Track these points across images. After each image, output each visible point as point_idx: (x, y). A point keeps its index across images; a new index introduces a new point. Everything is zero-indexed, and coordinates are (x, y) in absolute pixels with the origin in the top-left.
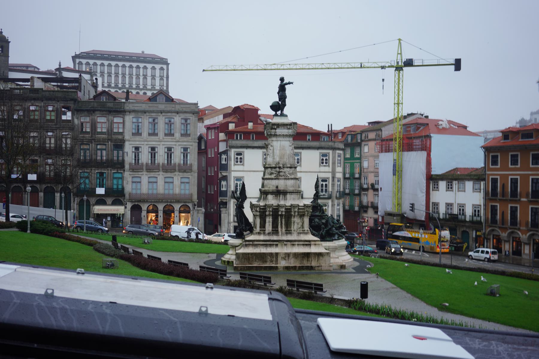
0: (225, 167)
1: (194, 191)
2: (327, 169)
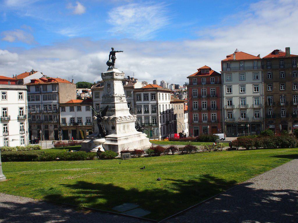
2: (21, 101)
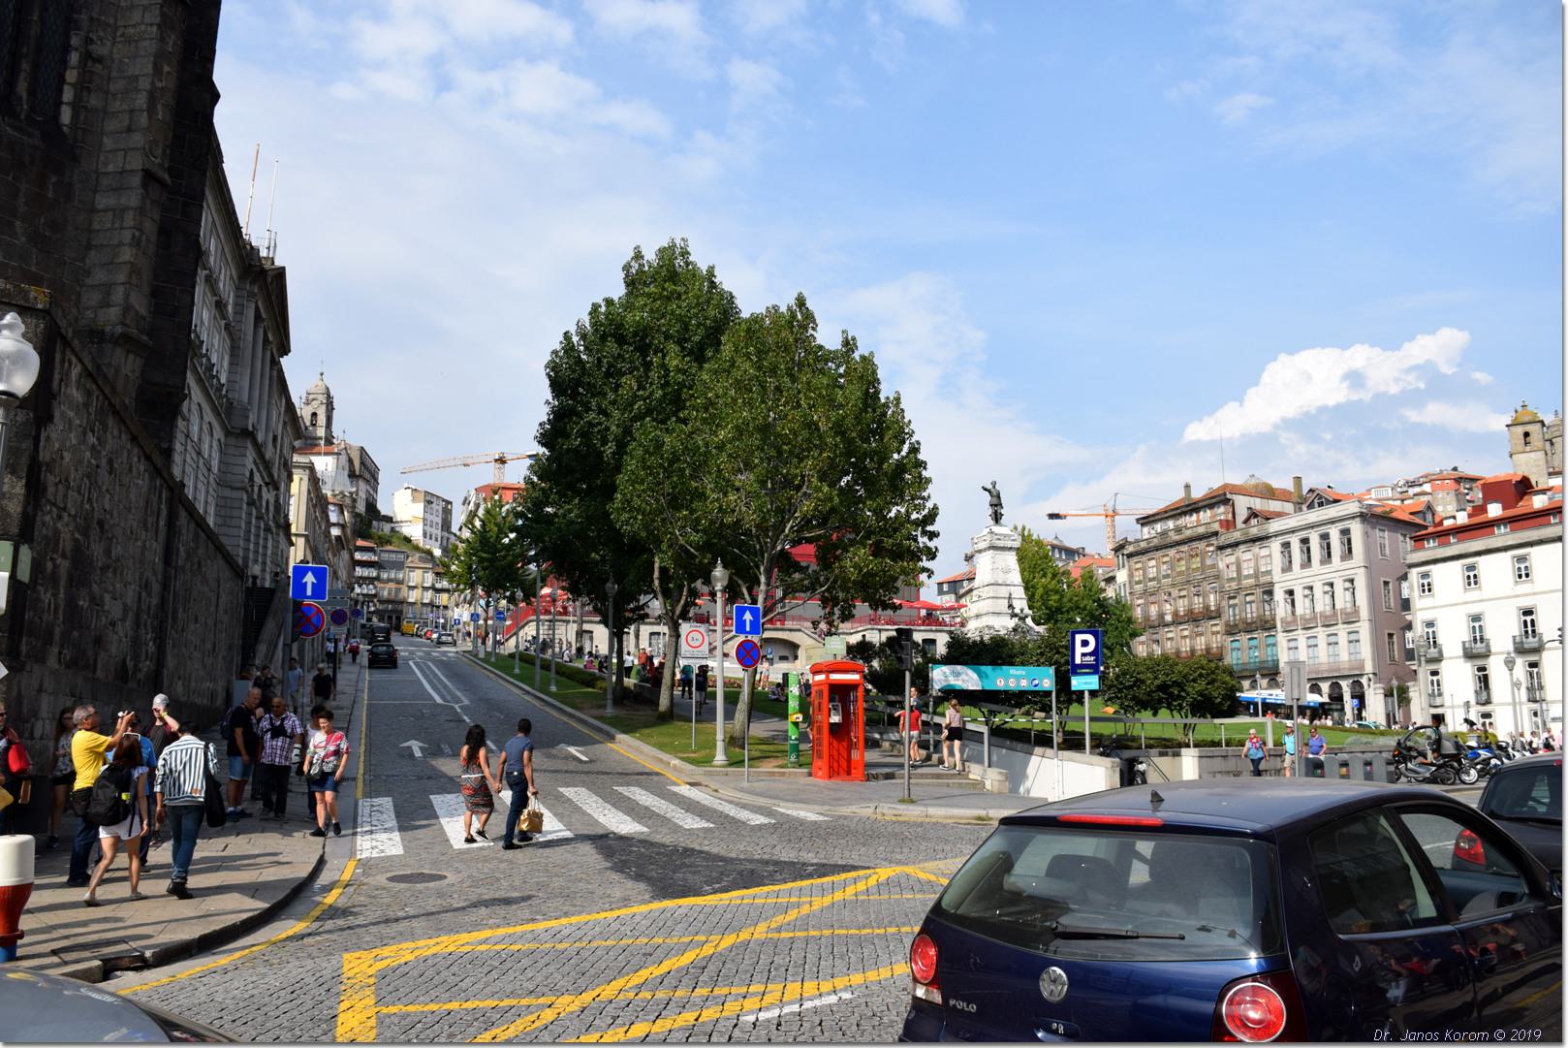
0: (1406, 605)
1: (1366, 651)
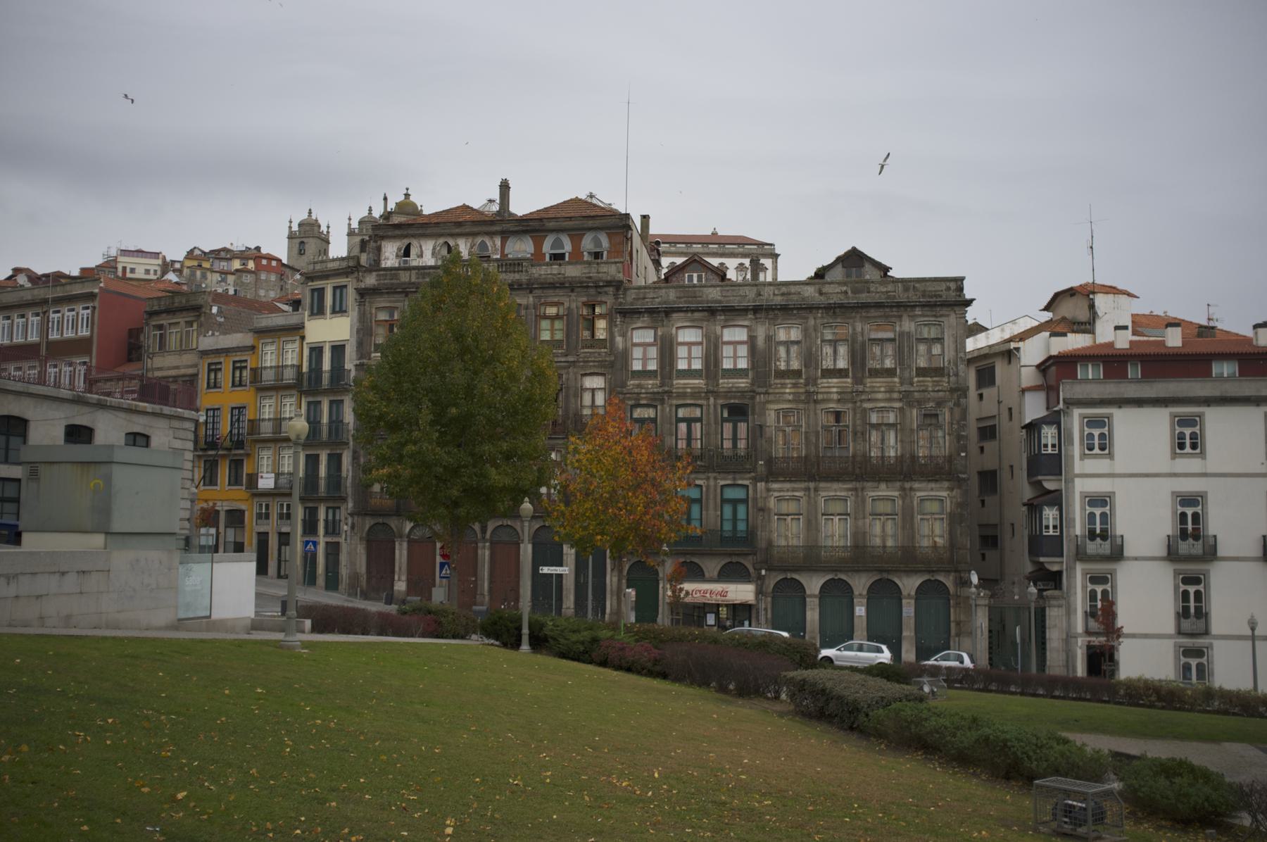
0: (1055, 464)
